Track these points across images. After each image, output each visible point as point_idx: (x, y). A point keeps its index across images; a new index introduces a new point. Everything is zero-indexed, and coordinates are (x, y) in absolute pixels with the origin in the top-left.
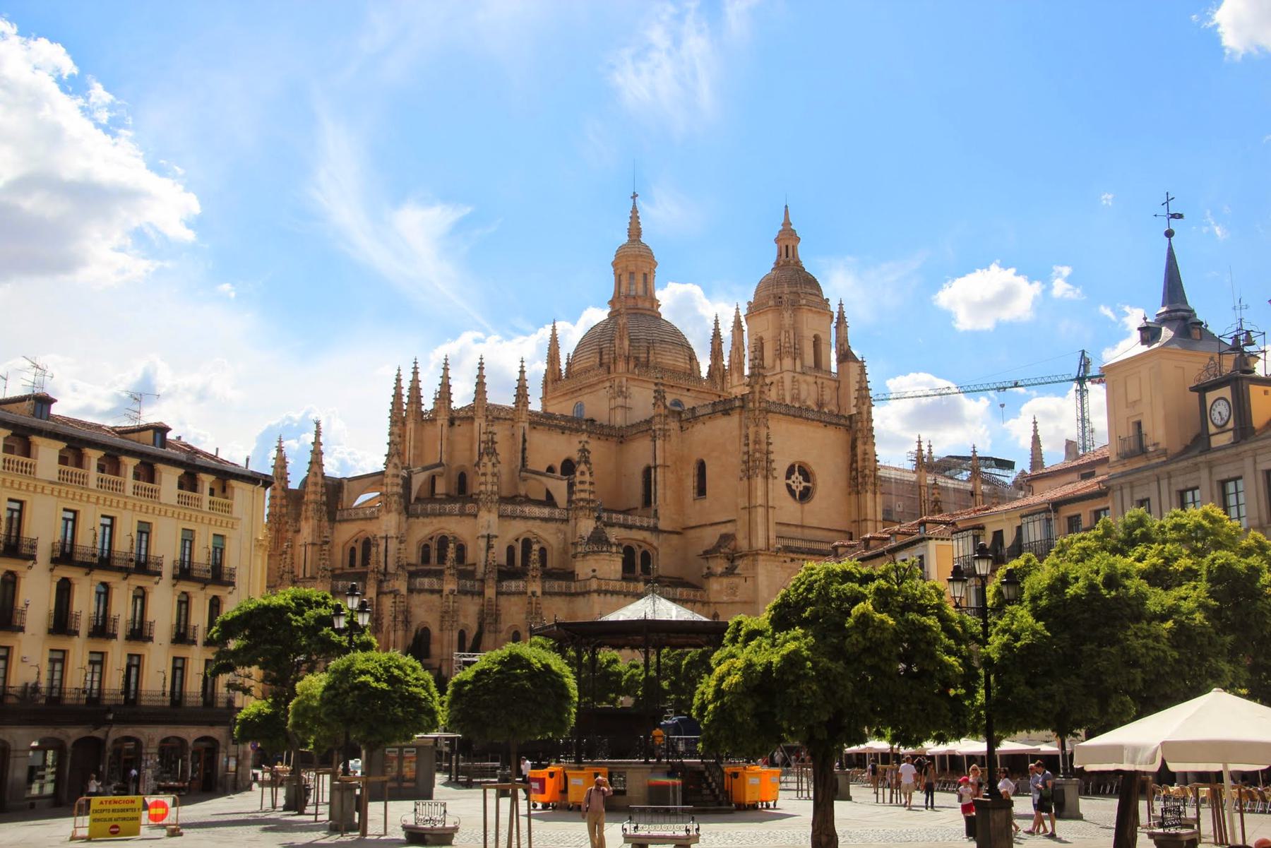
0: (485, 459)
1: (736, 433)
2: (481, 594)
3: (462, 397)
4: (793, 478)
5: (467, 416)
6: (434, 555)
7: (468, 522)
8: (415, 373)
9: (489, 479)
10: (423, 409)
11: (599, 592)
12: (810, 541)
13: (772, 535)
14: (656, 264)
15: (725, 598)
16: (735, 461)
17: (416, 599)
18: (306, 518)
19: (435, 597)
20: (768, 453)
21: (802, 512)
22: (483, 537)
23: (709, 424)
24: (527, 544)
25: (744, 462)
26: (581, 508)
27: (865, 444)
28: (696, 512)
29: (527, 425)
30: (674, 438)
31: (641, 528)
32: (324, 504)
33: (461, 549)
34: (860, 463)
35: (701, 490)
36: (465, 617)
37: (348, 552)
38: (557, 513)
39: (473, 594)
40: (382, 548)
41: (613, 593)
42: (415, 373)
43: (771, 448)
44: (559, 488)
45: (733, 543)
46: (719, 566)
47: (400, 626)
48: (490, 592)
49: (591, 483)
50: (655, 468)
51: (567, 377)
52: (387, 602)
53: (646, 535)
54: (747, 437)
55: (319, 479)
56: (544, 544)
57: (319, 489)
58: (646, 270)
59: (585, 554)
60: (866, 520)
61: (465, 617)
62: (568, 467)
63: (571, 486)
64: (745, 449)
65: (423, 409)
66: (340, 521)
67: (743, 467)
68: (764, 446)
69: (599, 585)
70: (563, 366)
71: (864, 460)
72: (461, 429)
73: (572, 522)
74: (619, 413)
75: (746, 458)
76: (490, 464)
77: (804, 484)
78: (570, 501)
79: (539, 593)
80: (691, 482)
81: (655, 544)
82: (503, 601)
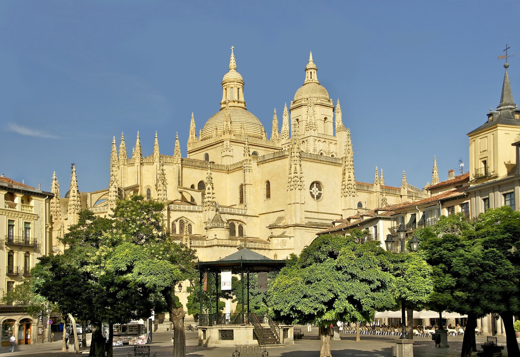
4: (313, 189)
12: (322, 219)
15: (280, 248)
21: (318, 205)
31: (238, 215)
38: (196, 208)
44: (197, 196)
46: (277, 232)
57: (76, 198)
62: (202, 185)
63: (203, 194)
81: (245, 222)
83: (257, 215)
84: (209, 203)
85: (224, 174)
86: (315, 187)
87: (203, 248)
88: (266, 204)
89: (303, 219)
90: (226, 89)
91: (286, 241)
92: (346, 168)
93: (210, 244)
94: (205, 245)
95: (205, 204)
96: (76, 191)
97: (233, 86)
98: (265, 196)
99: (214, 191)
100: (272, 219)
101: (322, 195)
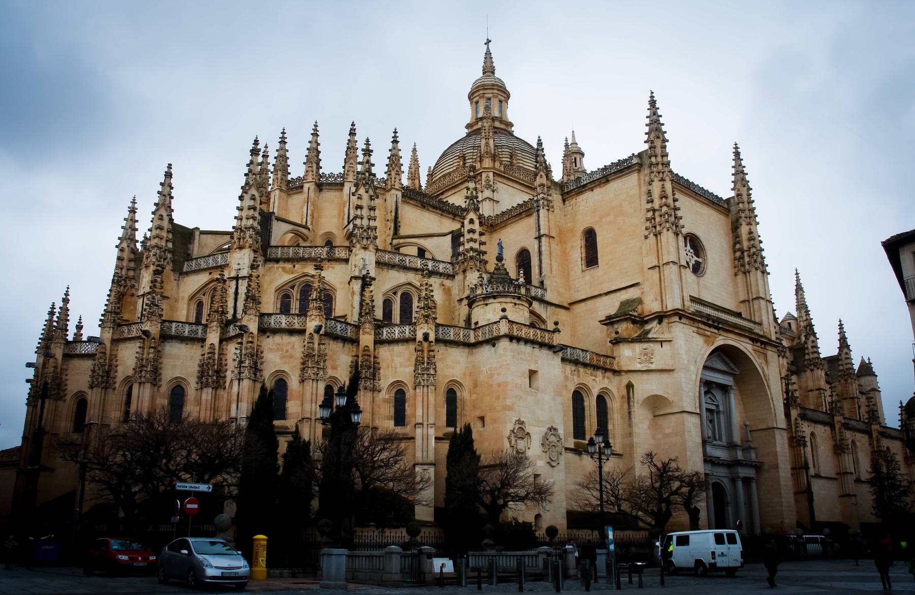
0: (362, 191)
1: (635, 191)
2: (355, 341)
3: (332, 163)
5: (336, 184)
6: (295, 307)
7: (339, 268)
8: (283, 142)
9: (365, 212)
10: (289, 177)
11: (511, 338)
13: (687, 298)
14: (508, 96)
15: (639, 367)
16: (637, 217)
18: (147, 267)
19: (295, 340)
20: (676, 209)
21: (698, 284)
22: (356, 278)
23: (597, 191)
24: (406, 300)
25: (647, 220)
26: (471, 258)
27: (749, 224)
28: (584, 283)
29: (399, 194)
30: (556, 211)
32: (169, 251)
33: (327, 299)
34: (746, 244)
35: (591, 260)
37: (194, 307)
39: (344, 340)
40: (232, 291)
41: (527, 341)
42: (283, 142)
45: (639, 307)
47: (246, 373)
48: (367, 339)
49: (481, 234)
50: (539, 238)
51: (430, 182)
52: (232, 350)
54: (649, 193)
55: (166, 224)
57: (164, 234)
58: (502, 98)
59: (485, 298)
60: (758, 298)
61: (335, 368)
64: (649, 206)
65: (289, 177)
66: (187, 273)
67: (648, 224)
68: (670, 201)
69: (511, 329)
70: (424, 183)
71: (750, 239)
72: (329, 195)
73: (459, 277)
75: (650, 214)
76: (366, 197)
77: (696, 258)
78: (455, 254)
80: (577, 253)
81: (544, 316)
82: (384, 352)
83: (566, 305)
84: (471, 254)
86: (689, 247)
87: (467, 350)
89: (688, 303)
90: (477, 102)
91: (653, 350)
92: (743, 215)
94: (472, 340)
95: (460, 258)
96: (166, 219)
97: (490, 95)
100: (609, 305)
101: (702, 266)
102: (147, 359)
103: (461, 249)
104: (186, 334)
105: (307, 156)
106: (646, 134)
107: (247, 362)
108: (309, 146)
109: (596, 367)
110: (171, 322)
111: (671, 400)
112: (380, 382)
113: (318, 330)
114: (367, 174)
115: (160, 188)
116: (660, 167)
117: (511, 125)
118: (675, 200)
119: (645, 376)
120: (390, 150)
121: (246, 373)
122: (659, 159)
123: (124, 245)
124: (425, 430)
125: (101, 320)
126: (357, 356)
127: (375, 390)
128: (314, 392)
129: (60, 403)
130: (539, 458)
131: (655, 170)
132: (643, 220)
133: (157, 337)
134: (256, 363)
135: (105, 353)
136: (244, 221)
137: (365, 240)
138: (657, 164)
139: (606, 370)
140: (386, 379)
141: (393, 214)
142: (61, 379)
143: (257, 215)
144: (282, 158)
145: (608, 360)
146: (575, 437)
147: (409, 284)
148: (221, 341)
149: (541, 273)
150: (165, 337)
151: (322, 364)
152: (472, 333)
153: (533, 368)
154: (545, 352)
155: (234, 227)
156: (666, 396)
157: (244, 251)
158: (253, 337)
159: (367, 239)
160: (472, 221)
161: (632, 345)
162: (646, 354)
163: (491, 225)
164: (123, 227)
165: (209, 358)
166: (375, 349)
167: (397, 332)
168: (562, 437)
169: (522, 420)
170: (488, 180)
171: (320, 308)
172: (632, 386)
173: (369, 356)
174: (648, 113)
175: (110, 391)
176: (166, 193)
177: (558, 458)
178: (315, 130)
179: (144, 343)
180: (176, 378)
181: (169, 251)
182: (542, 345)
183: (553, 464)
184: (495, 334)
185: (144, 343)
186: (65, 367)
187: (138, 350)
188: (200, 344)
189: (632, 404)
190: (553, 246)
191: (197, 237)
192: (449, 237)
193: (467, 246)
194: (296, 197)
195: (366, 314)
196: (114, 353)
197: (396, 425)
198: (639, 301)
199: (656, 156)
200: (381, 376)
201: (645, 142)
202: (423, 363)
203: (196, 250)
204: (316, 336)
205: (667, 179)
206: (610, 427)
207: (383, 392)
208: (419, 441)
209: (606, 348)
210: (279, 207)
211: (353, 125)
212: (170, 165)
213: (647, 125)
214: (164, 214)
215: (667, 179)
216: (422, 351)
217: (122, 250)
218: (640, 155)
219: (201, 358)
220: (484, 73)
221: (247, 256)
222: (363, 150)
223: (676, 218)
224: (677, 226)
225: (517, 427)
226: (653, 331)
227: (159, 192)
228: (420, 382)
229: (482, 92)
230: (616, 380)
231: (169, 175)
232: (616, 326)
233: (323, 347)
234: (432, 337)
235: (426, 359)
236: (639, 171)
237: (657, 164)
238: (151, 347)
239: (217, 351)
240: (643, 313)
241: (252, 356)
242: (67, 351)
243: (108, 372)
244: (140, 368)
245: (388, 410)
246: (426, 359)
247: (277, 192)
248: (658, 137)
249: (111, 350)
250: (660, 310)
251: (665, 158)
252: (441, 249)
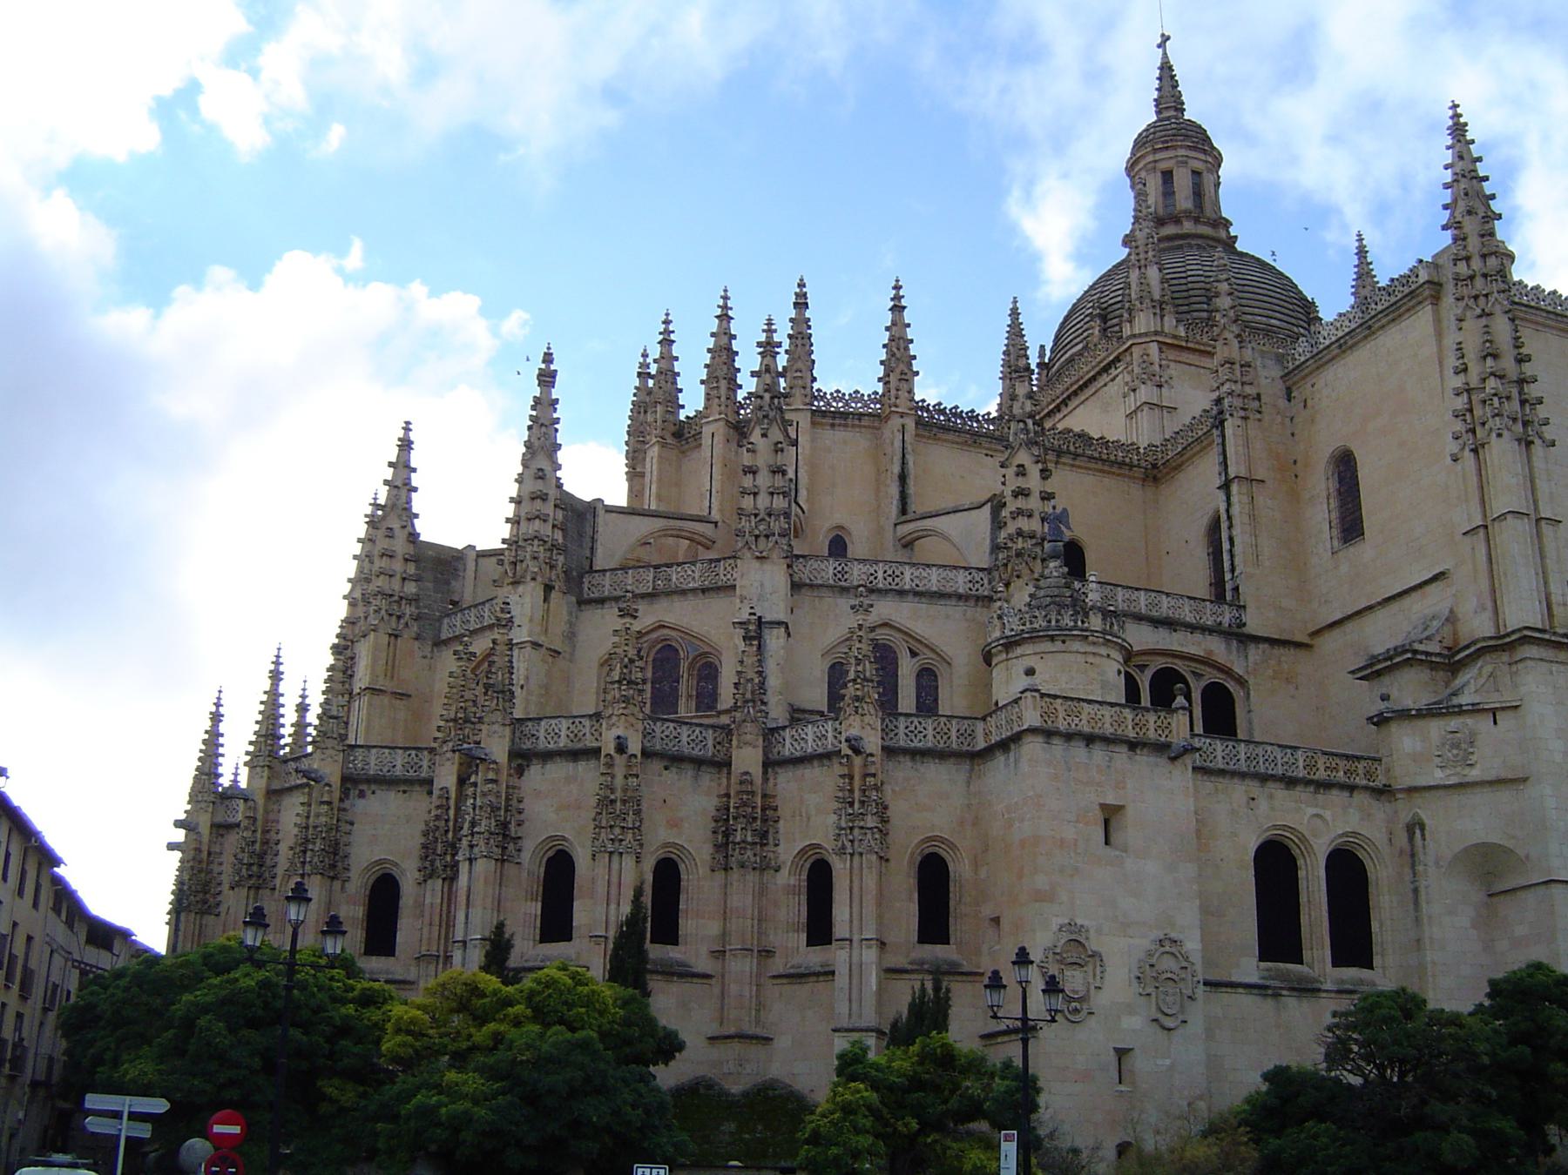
1: (1430, 349)
2: (724, 765)
7: (718, 604)
8: (667, 342)
9: (764, 480)
10: (682, 416)
11: (1048, 734)
15: (1439, 776)
16: (1436, 416)
17: (537, 777)
20: (1522, 382)
24: (885, 658)
26: (1019, 554)
29: (910, 424)
30: (1266, 418)
31: (1192, 628)
32: (410, 601)
33: (708, 672)
35: (1351, 527)
36: (674, 824)
39: (699, 763)
41: (1090, 740)
43: (1528, 369)
46: (1410, 689)
47: (481, 848)
48: (747, 758)
49: (1047, 497)
53: (1216, 648)
55: (400, 546)
56: (926, 657)
57: (398, 566)
58: (1198, 166)
59: (1010, 644)
65: (682, 416)
67: (1459, 426)
68: (1508, 364)
74: (1144, 417)
75: (1460, 403)
78: (996, 548)
79: (872, 742)
80: (1321, 514)
82: (786, 783)
83: (1299, 638)
84: (1020, 544)
85: (1135, 490)
88: (1344, 568)
93: (1006, 734)
94: (981, 744)
96: (401, 536)
98: (1335, 532)
99: (1049, 486)
102: (315, 827)
103: (1003, 534)
104: (399, 771)
105: (707, 366)
106: (1446, 207)
107: (484, 823)
108: (711, 343)
109: (1325, 786)
110: (369, 747)
111: (1521, 853)
112: (780, 849)
113: (621, 747)
114: (767, 396)
115: (389, 474)
116: (1479, 282)
117: (1227, 224)
118: (1521, 360)
119: (1455, 799)
120: (887, 329)
121: (481, 848)
122: (1476, 264)
123: (358, 595)
124: (855, 953)
125: (247, 753)
126: (728, 795)
127: (766, 867)
128: (615, 879)
129: (209, 920)
130: (1130, 1010)
131: (1465, 291)
132: (1449, 416)
133: (336, 780)
134: (505, 825)
135: (255, 819)
136: (523, 524)
137: (762, 539)
138: (1472, 278)
139: (1352, 789)
140: (789, 846)
141: (896, 469)
142: (211, 872)
143: (548, 509)
144: (668, 375)
145: (1361, 766)
146: (1264, 956)
147: (885, 625)
148: (462, 781)
149: (1233, 570)
150: (353, 783)
151: (630, 818)
152: (980, 726)
153: (1110, 800)
154: (1143, 759)
155: (504, 541)
156: (1509, 844)
157: (521, 588)
158: (497, 771)
159: (767, 536)
160: (1021, 471)
161: (1421, 723)
162: (1456, 745)
163: (1154, 466)
164: (355, 557)
165: (437, 817)
166: (766, 780)
167: (810, 738)
168: (1196, 958)
169: (1079, 922)
170: (1146, 362)
171: (626, 700)
172: (1422, 827)
173: (753, 793)
174: (1448, 157)
175: (265, 893)
176: (398, 483)
177: (1182, 1009)
178: (725, 307)
179: (310, 794)
180: (379, 862)
181: (410, 601)
182: (1133, 746)
183: (1169, 1023)
184: (1016, 729)
185: (310, 794)
186: (217, 849)
187: (300, 809)
188: (426, 788)
189: (1420, 868)
190: (1260, 500)
191: (471, 566)
192: (987, 508)
193: (1011, 528)
194: (695, 455)
195: (747, 701)
196: (272, 816)
197: (811, 942)
198: (1452, 619)
199: (1468, 259)
200: (781, 837)
201: (1445, 228)
202: (851, 804)
203: (467, 590)
204: (620, 760)
205: (1498, 309)
206: (1375, 926)
207: (785, 872)
208: (841, 980)
209: (1362, 739)
210: (660, 480)
211: (802, 285)
212: (408, 423)
213: (1447, 186)
214: (396, 525)
215: (1498, 309)
216: (851, 777)
217: (353, 604)
218: (1435, 265)
219: (427, 817)
220: (1158, 113)
221: (527, 599)
222: (759, 344)
223: (1523, 402)
224: (1525, 424)
225: (1065, 937)
226: (1472, 687)
227: (386, 482)
228: (844, 847)
229: (1150, 158)
230: (1380, 811)
231: (406, 445)
232: (1386, 679)
233: (633, 781)
234: (872, 742)
235: (857, 794)
236: (1436, 299)
237: (1472, 278)
238: (323, 803)
239: (452, 803)
240: (1456, 641)
241: (495, 809)
242: (219, 819)
243: (262, 855)
244: (304, 845)
245: (794, 909)
246: (857, 794)
247: (656, 449)
248: (1469, 213)
249: (266, 812)
250: (1490, 632)
251: (1492, 262)
252: (969, 536)
